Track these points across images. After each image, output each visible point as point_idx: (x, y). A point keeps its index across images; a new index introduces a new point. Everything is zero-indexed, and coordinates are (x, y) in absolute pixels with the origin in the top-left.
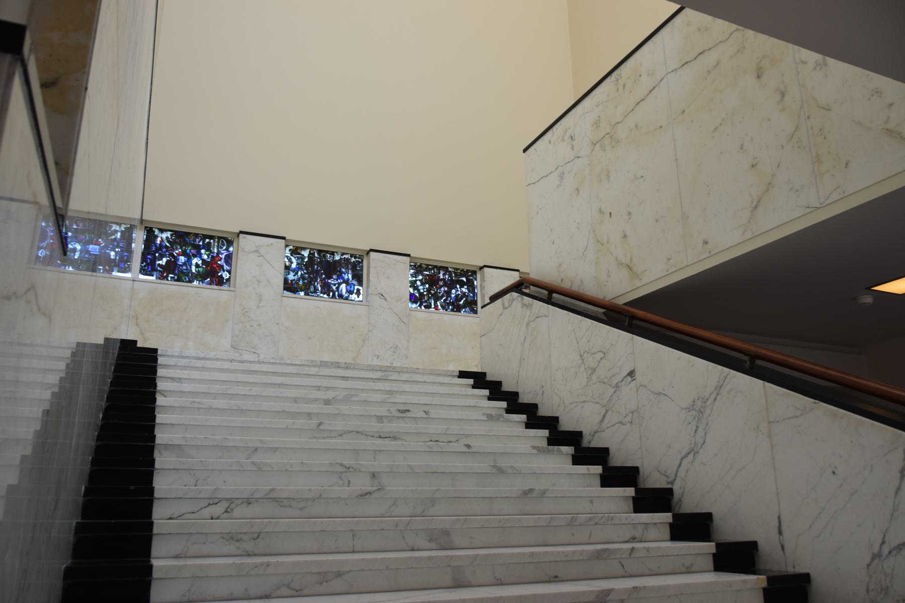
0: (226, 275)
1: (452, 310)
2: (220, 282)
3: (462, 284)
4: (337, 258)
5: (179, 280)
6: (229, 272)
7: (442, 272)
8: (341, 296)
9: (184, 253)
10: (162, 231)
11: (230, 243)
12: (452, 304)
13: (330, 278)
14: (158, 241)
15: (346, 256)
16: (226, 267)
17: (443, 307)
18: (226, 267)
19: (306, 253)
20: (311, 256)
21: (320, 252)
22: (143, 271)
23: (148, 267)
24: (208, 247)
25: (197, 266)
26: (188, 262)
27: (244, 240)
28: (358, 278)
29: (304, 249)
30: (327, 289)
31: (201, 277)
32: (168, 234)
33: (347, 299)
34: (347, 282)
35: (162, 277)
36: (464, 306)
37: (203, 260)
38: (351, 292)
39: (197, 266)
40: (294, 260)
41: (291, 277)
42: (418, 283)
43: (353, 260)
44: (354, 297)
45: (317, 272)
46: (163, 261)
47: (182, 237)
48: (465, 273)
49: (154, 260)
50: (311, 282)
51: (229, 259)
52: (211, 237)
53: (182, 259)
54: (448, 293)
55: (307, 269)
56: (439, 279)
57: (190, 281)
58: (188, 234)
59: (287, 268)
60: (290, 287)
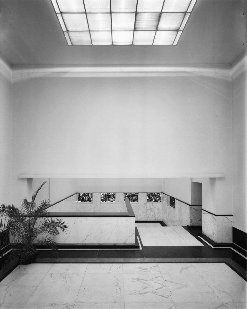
0: (92, 200)
1: (133, 201)
2: (91, 201)
3: (135, 196)
4: (110, 194)
5: (84, 202)
6: (92, 199)
7: (131, 194)
8: (111, 201)
9: (85, 197)
10: (81, 193)
11: (92, 194)
12: (133, 200)
13: (109, 198)
14: (81, 195)
15: (112, 194)
16: (92, 198)
17: (131, 201)
18: (92, 198)
19: (105, 194)
20: (106, 195)
21: (107, 193)
22: (79, 201)
23: (79, 200)
24: (88, 195)
25: (87, 199)
26: (86, 198)
27: (94, 194)
28: (114, 197)
29: (104, 193)
30: (109, 200)
31: (88, 200)
32: (82, 194)
33: (112, 202)
34: (112, 199)
35: (82, 201)
36: (135, 200)
37: (88, 198)
38: (113, 200)
39: (87, 199)
40: (103, 195)
41: (102, 199)
42: (126, 197)
43: (113, 194)
44: (114, 201)
45: (107, 197)
46: (82, 199)
47: (84, 194)
48: (136, 194)
49: (80, 199)
50: (106, 199)
51: (92, 197)
52: (89, 193)
53: (85, 198)
54: (132, 198)
55: (105, 197)
56: (130, 196)
57: (86, 202)
58: (85, 193)
59: (102, 197)
60: (102, 201)
